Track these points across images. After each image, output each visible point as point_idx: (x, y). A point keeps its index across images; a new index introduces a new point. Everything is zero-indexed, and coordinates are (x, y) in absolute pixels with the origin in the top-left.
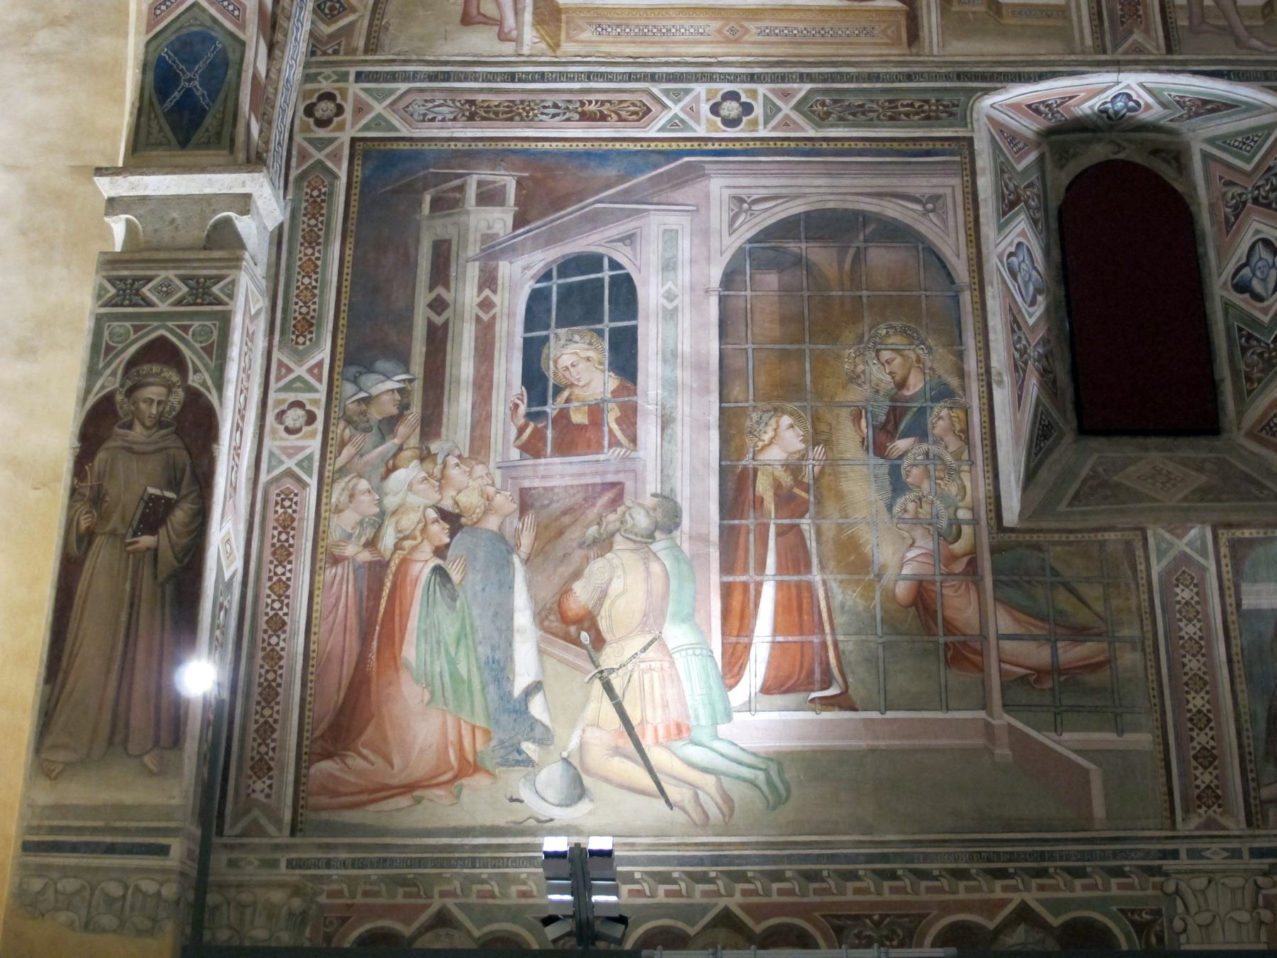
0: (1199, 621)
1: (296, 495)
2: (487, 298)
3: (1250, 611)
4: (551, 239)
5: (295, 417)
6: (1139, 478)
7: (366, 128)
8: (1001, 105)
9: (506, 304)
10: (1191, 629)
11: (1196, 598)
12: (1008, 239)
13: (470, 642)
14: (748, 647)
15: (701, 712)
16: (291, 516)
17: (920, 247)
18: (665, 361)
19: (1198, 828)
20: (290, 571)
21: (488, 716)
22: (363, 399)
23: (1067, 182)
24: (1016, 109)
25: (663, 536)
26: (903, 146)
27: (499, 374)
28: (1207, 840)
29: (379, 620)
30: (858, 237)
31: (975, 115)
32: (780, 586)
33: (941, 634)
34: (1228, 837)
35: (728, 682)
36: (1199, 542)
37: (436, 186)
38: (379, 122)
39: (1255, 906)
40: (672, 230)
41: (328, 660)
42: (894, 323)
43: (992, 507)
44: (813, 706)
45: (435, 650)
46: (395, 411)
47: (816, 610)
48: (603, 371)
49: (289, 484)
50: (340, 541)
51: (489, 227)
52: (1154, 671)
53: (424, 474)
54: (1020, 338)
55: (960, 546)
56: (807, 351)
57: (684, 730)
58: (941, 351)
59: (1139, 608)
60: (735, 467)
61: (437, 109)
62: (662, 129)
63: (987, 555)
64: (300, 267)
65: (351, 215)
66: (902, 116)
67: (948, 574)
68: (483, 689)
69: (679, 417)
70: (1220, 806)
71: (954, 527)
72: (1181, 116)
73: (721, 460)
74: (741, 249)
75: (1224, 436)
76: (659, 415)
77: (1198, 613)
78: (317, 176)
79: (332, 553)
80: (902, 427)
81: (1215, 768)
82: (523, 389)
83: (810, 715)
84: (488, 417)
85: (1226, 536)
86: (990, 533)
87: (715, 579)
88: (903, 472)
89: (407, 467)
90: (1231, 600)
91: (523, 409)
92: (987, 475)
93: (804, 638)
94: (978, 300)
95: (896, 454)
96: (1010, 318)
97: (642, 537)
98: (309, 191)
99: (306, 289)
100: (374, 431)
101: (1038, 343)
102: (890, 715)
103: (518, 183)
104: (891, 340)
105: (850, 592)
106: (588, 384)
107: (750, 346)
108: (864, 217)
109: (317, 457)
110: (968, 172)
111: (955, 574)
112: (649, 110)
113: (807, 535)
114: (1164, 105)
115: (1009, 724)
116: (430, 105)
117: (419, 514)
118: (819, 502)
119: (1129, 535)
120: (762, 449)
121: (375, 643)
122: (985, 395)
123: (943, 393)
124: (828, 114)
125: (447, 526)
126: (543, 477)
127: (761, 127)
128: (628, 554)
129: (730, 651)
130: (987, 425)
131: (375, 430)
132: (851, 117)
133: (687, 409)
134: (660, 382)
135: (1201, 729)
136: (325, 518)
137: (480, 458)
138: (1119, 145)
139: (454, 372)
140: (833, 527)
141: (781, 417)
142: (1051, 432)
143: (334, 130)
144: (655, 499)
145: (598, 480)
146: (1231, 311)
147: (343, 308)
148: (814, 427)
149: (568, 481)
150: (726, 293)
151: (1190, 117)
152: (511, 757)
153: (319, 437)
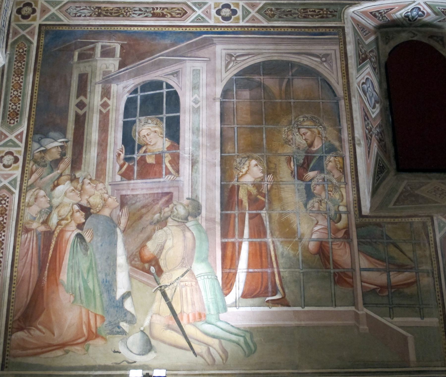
1: (8, 198)
2: (105, 102)
4: (137, 74)
5: (8, 159)
6: (428, 192)
7: (47, 19)
8: (357, 12)
9: (115, 104)
12: (362, 76)
13: (94, 271)
14: (235, 274)
15: (211, 307)
16: (5, 208)
17: (319, 78)
18: (193, 133)
20: (4, 236)
21: (103, 309)
22: (43, 151)
23: (388, 50)
24: (365, 15)
25: (192, 219)
26: (310, 30)
27: (111, 139)
29: (49, 260)
30: (289, 73)
31: (345, 16)
32: (251, 244)
33: (332, 268)
35: (225, 292)
37: (81, 47)
38: (53, 17)
40: (197, 70)
41: (23, 280)
42: (307, 115)
43: (356, 205)
44: (268, 304)
45: (77, 276)
46: (58, 157)
47: (269, 256)
48: (163, 138)
49: (5, 192)
50: (30, 221)
51: (107, 68)
53: (72, 188)
54: (368, 123)
55: (340, 225)
56: (264, 128)
57: (203, 316)
58: (330, 129)
59: (430, 255)
60: (229, 184)
61: (82, 11)
62: (192, 21)
63: (354, 229)
64: (13, 86)
65: (38, 61)
66: (310, 17)
67: (335, 238)
68: (101, 295)
69: (200, 160)
71: (338, 215)
73: (221, 181)
74: (231, 79)
76: (191, 159)
78: (22, 43)
79: (26, 227)
80: (311, 165)
82: (123, 146)
83: (266, 309)
84: (105, 160)
86: (355, 218)
87: (218, 240)
88: (312, 188)
89: (64, 184)
91: (122, 156)
92: (354, 189)
93: (264, 270)
94: (347, 104)
95: (308, 179)
96: (363, 113)
97: (182, 219)
98: (18, 49)
99: (15, 97)
100: (48, 167)
101: (377, 126)
102: (306, 309)
103: (122, 46)
104: (305, 124)
105: (286, 247)
106: (155, 144)
107: (236, 126)
108: (291, 64)
109: (19, 179)
110: (342, 43)
111: (339, 238)
112: (186, 12)
113: (264, 219)
115: (367, 313)
116: (78, 9)
117: (70, 208)
118: (270, 202)
119: (425, 219)
120: (242, 176)
121: (46, 272)
122: (352, 150)
123: (331, 149)
124: (274, 15)
125: (84, 214)
126: (132, 190)
127: (241, 21)
128: (175, 228)
129: (226, 276)
130: (353, 165)
131: (48, 166)
132: (285, 17)
133: (204, 156)
134: (191, 143)
136: (22, 210)
137: (101, 180)
138: (414, 34)
139: (88, 137)
140: (278, 215)
141: (251, 160)
142: (384, 169)
143: (31, 21)
144: (189, 201)
145: (160, 191)
147: (33, 106)
148: (268, 166)
149: (145, 192)
150: (224, 100)
152: (114, 330)
153: (20, 169)
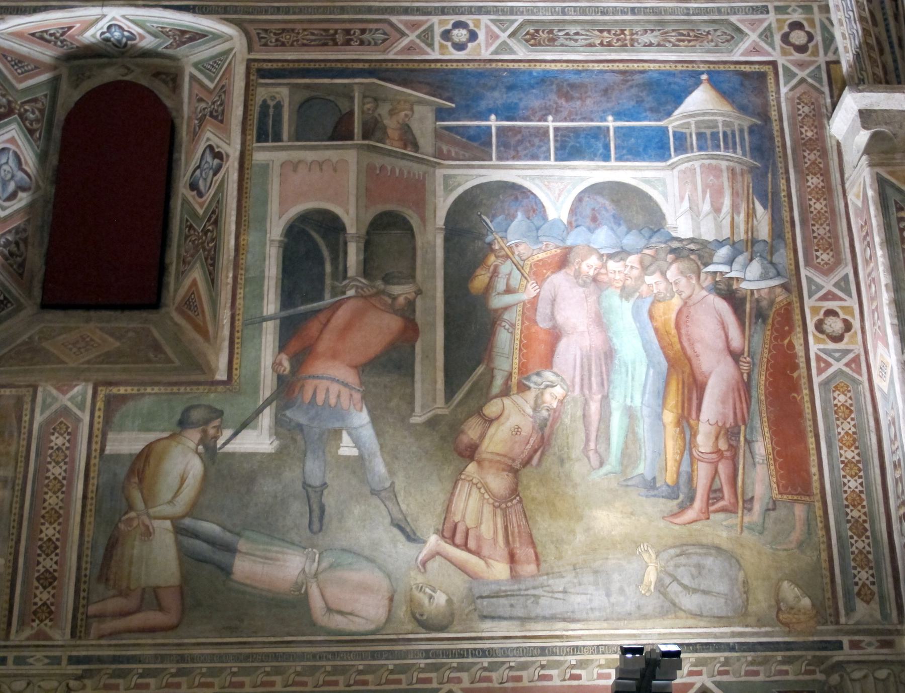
0: (66, 463)
3: (111, 456)
11: (67, 445)
19: (28, 639)
28: (34, 649)
34: (53, 646)
36: (80, 398)
52: (18, 506)
70: (51, 620)
72: (171, 44)
75: (163, 310)
77: (66, 456)
81: (54, 588)
90: (96, 446)
114: (155, 35)
119: (23, 391)
135: (48, 555)
138: (128, 69)
142: (6, 305)
151: (179, 46)
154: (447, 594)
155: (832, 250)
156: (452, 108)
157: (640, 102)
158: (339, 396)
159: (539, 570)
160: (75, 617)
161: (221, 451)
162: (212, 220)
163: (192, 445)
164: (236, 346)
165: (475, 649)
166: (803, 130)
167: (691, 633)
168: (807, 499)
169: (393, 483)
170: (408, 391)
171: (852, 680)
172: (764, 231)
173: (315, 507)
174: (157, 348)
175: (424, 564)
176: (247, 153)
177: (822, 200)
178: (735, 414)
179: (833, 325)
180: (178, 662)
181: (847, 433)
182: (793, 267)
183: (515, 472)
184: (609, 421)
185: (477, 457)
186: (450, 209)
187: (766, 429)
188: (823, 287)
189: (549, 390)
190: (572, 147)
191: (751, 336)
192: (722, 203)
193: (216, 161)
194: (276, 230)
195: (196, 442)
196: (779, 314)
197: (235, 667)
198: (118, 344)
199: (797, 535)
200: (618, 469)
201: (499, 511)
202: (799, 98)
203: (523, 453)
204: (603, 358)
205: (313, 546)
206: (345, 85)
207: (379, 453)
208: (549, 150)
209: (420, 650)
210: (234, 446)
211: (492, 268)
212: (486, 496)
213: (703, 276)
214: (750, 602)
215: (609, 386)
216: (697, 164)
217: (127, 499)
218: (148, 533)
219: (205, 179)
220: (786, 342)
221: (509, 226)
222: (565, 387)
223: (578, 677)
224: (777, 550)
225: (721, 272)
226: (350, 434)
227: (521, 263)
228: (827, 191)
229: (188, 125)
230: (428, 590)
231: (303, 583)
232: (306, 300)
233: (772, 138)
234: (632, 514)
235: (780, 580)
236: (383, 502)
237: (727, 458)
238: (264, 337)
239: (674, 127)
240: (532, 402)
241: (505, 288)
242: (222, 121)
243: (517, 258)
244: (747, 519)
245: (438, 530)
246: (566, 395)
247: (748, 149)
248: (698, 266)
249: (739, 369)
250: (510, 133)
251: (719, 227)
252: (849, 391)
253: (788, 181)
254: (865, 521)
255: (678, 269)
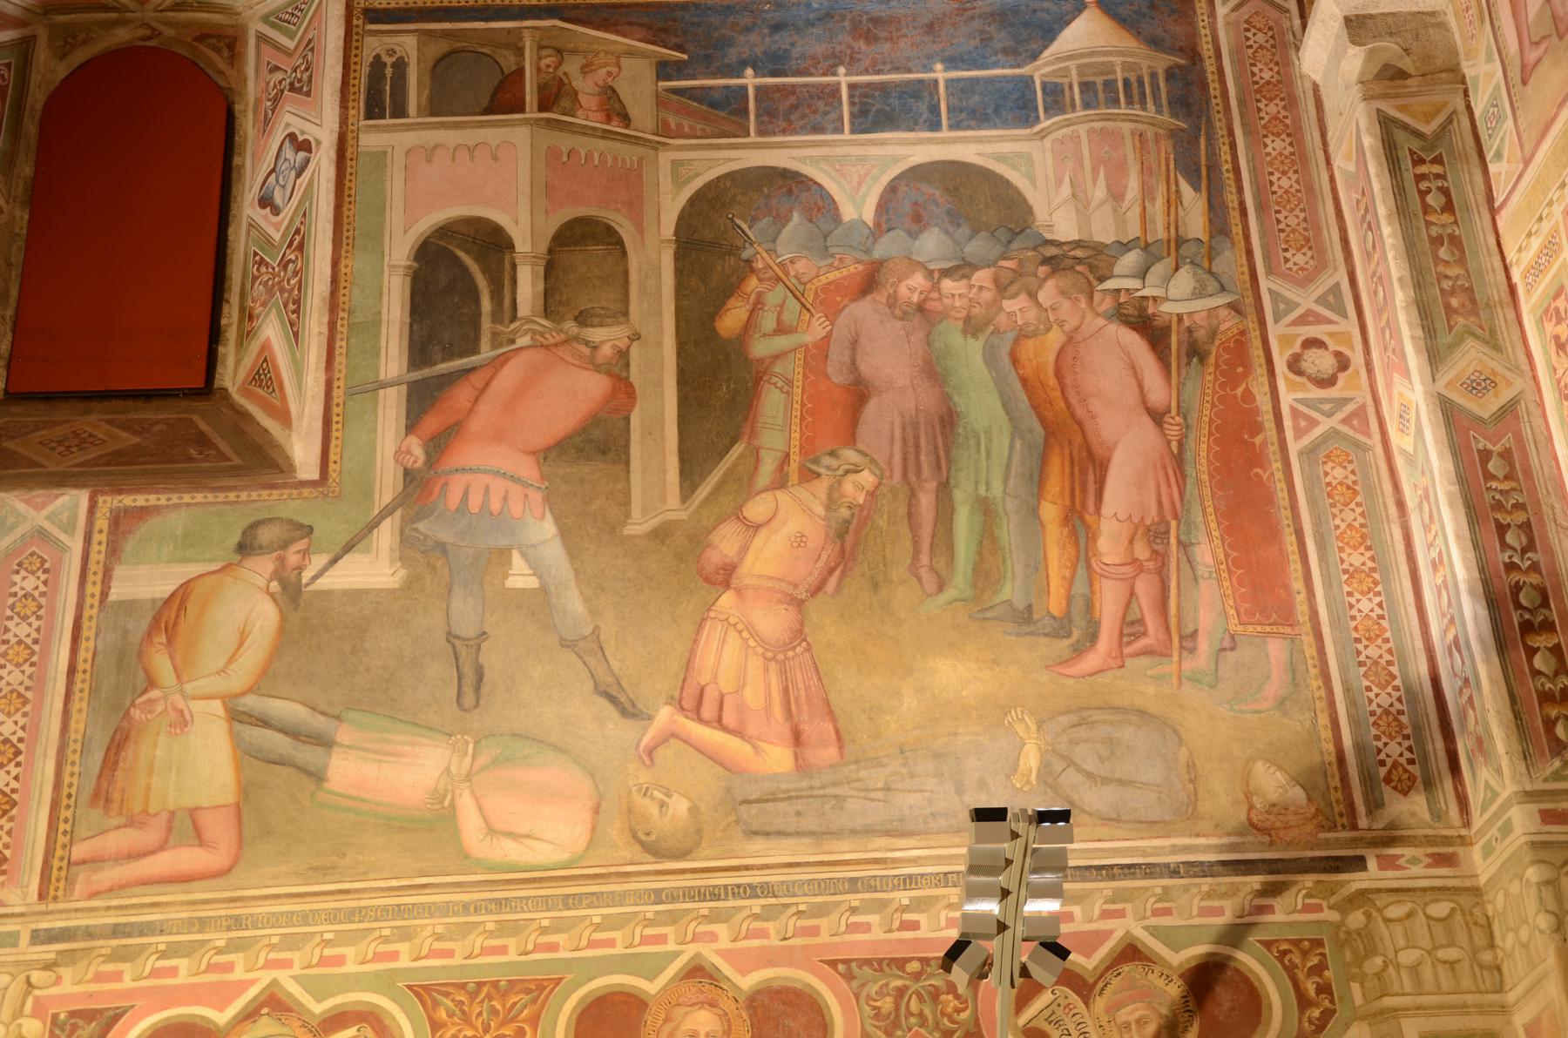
0: (39, 618)
3: (120, 603)
10: (23, 630)
11: (42, 588)
36: (66, 514)
39: (18, 1013)
77: (40, 607)
85: (109, 505)
90: (93, 589)
146: (254, 233)
154: (690, 800)
155: (1310, 248)
156: (684, 62)
157: (986, 40)
158: (505, 499)
159: (842, 756)
160: (46, 865)
161: (309, 588)
162: (296, 243)
163: (261, 582)
164: (335, 426)
165: (738, 886)
166: (1256, 70)
167: (1102, 850)
168: (1288, 630)
169: (596, 629)
170: (620, 486)
171: (1387, 921)
172: (1196, 222)
173: (468, 670)
174: (202, 441)
175: (650, 752)
176: (350, 135)
177: (1290, 174)
178: (1160, 503)
179: (1317, 362)
180: (229, 929)
181: (1350, 526)
182: (1247, 277)
183: (800, 604)
184: (952, 520)
185: (734, 582)
186: (683, 211)
187: (1213, 525)
188: (1298, 305)
189: (851, 477)
190: (878, 112)
191: (1181, 385)
192: (1126, 187)
193: (302, 154)
194: (400, 249)
195: (267, 576)
196: (1225, 349)
197: (329, 931)
198: (136, 440)
199: (1275, 686)
200: (968, 593)
201: (773, 666)
202: (1247, 22)
203: (810, 574)
204: (938, 427)
205: (464, 731)
206: (509, 31)
207: (573, 583)
208: (841, 118)
209: (646, 890)
210: (330, 580)
211: (753, 297)
212: (752, 643)
213: (1097, 297)
214: (1200, 797)
215: (949, 470)
216: (1082, 130)
217: (146, 671)
218: (182, 722)
219: (283, 187)
220: (1240, 391)
221: (779, 232)
222: (877, 472)
223: (915, 926)
224: (1241, 711)
225: (1127, 290)
226: (524, 555)
227: (801, 288)
228: (1299, 159)
229: (255, 112)
230: (657, 794)
231: (446, 791)
232: (449, 355)
233: (1204, 86)
234: (994, 662)
235: (1250, 760)
236: (580, 657)
237: (1149, 572)
238: (380, 412)
239: (1043, 75)
240: (823, 497)
241: (774, 325)
242: (308, 94)
243: (793, 280)
244: (1187, 665)
245: (672, 698)
246: (880, 484)
247: (1165, 102)
248: (1089, 281)
249: (1164, 435)
250: (777, 95)
251: (1121, 221)
252: (1351, 462)
253: (1233, 146)
254: (1390, 663)
255: (1057, 287)
